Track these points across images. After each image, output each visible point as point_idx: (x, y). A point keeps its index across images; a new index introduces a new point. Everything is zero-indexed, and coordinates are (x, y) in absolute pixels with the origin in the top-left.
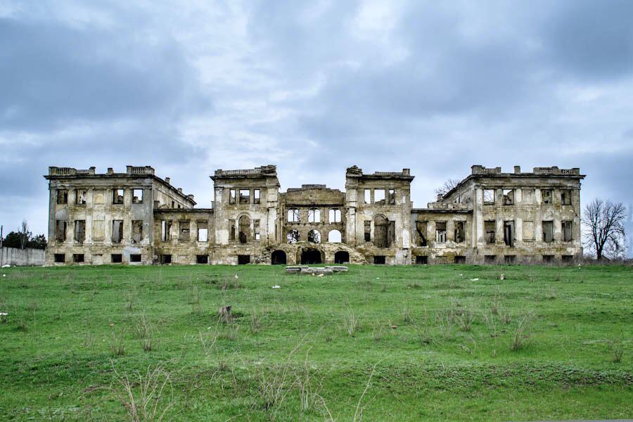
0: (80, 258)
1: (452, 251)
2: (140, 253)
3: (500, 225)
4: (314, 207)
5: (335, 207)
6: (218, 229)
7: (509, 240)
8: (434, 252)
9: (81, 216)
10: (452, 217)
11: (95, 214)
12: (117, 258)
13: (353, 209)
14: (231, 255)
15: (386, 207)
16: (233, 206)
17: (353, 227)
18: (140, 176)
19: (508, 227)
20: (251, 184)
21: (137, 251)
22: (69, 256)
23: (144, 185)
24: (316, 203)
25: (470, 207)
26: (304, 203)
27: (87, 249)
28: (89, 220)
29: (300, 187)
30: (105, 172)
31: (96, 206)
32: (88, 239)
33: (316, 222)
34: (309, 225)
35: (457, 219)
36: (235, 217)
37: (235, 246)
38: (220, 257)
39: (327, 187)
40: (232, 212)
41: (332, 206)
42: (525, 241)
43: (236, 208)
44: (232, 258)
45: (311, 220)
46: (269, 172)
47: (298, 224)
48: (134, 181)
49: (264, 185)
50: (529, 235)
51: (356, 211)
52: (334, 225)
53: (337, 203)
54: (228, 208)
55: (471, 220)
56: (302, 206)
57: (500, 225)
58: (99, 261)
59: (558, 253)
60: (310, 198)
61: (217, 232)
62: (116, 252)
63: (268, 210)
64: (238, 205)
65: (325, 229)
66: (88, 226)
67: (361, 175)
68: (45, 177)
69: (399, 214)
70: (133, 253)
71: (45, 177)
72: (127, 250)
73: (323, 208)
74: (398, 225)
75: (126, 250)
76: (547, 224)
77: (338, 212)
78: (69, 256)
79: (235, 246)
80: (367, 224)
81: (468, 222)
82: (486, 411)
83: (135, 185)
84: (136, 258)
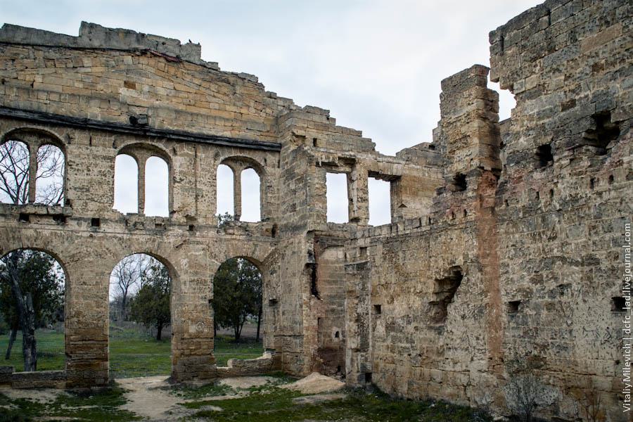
4: (140, 136)
5: (242, 153)
24: (155, 123)
26: (95, 112)
29: (75, 32)
33: (149, 212)
34: (119, 229)
41: (233, 143)
45: (125, 203)
47: (61, 219)
52: (239, 235)
53: (251, 136)
56: (84, 125)
60: (124, 92)
65: (197, 252)
73: (188, 150)
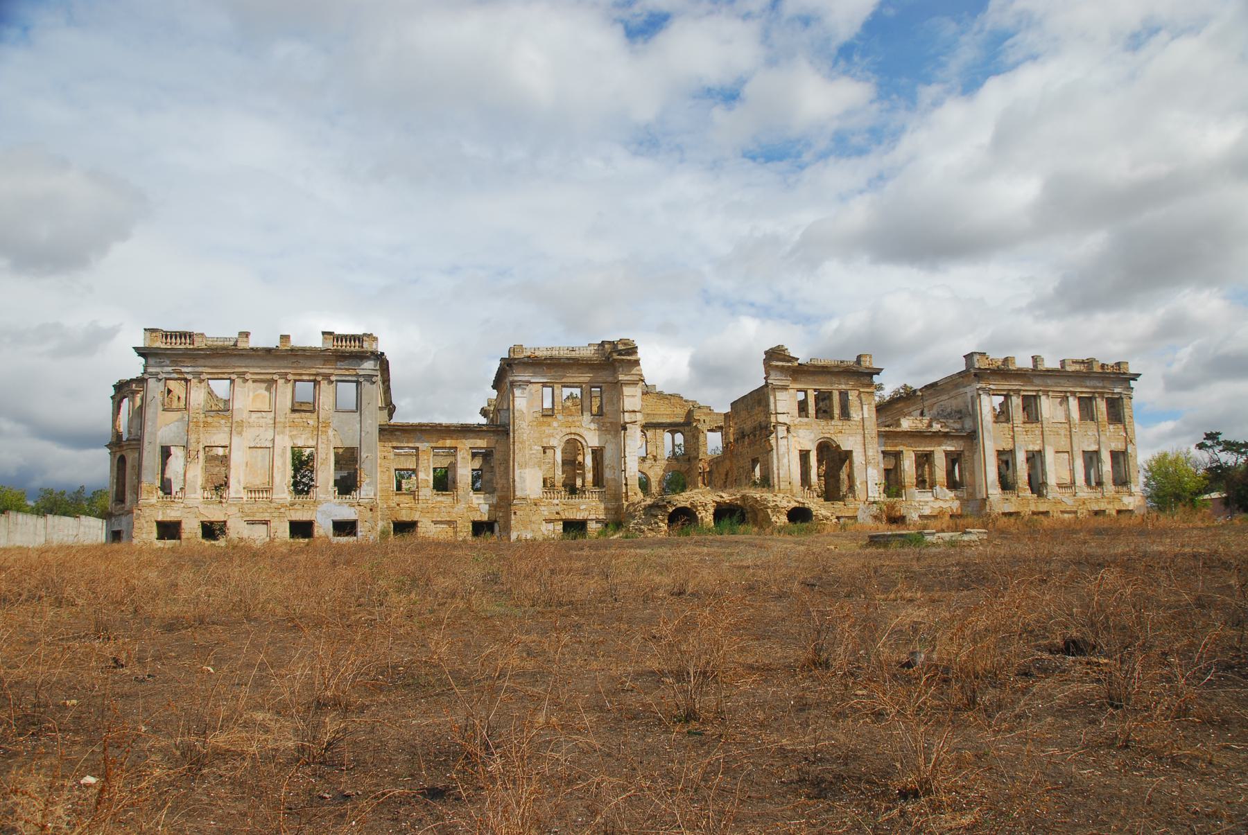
0: (211, 530)
1: (945, 505)
2: (353, 517)
3: (1021, 457)
5: (673, 428)
6: (521, 467)
7: (1037, 486)
8: (916, 509)
9: (219, 438)
10: (940, 445)
13: (785, 428)
14: (548, 521)
15: (837, 422)
16: (549, 419)
17: (785, 461)
18: (352, 356)
19: (1035, 458)
20: (585, 377)
21: (346, 513)
22: (191, 528)
23: (361, 372)
25: (967, 426)
27: (233, 510)
30: (273, 342)
31: (254, 415)
35: (949, 448)
36: (554, 442)
37: (556, 501)
38: (525, 524)
39: (658, 390)
40: (548, 430)
41: (670, 425)
42: (1060, 486)
43: (555, 424)
44: (551, 526)
46: (629, 354)
49: (610, 379)
50: (1067, 479)
51: (788, 430)
54: (541, 424)
57: (1021, 457)
58: (258, 535)
59: (1110, 507)
61: (517, 472)
63: (625, 429)
64: (560, 417)
66: (237, 458)
67: (796, 364)
68: (136, 349)
69: (859, 438)
70: (338, 518)
71: (136, 349)
74: (858, 458)
75: (324, 513)
76: (1092, 458)
77: (679, 438)
78: (191, 528)
79: (556, 501)
80: (804, 455)
81: (966, 453)
82: (916, 795)
84: (344, 528)
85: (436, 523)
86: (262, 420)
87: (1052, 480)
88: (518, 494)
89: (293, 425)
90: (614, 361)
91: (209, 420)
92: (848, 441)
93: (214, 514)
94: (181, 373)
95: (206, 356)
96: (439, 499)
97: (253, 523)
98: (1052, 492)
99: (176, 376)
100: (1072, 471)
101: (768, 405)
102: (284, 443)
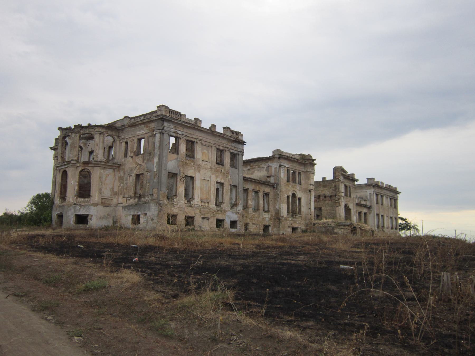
2: (237, 219)
9: (190, 173)
11: (203, 171)
12: (220, 223)
14: (289, 227)
21: (235, 217)
22: (181, 219)
28: (198, 177)
31: (204, 163)
32: (197, 201)
48: (232, 144)
55: (370, 213)
62: (220, 217)
66: (198, 183)
70: (232, 219)
72: (230, 216)
75: (228, 216)
78: (181, 219)
83: (233, 148)
85: (254, 224)
86: (207, 166)
87: (386, 226)
88: (282, 214)
89: (217, 171)
90: (307, 162)
91: (187, 162)
92: (351, 206)
93: (190, 212)
94: (177, 133)
95: (189, 128)
96: (254, 213)
97: (203, 218)
98: (386, 230)
99: (174, 134)
100: (388, 223)
101: (339, 189)
102: (214, 179)
